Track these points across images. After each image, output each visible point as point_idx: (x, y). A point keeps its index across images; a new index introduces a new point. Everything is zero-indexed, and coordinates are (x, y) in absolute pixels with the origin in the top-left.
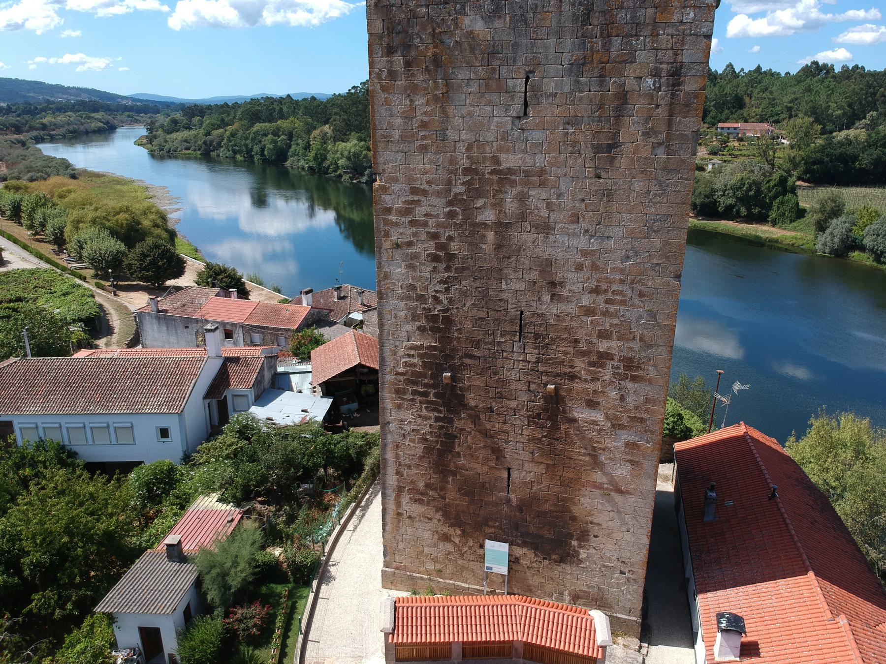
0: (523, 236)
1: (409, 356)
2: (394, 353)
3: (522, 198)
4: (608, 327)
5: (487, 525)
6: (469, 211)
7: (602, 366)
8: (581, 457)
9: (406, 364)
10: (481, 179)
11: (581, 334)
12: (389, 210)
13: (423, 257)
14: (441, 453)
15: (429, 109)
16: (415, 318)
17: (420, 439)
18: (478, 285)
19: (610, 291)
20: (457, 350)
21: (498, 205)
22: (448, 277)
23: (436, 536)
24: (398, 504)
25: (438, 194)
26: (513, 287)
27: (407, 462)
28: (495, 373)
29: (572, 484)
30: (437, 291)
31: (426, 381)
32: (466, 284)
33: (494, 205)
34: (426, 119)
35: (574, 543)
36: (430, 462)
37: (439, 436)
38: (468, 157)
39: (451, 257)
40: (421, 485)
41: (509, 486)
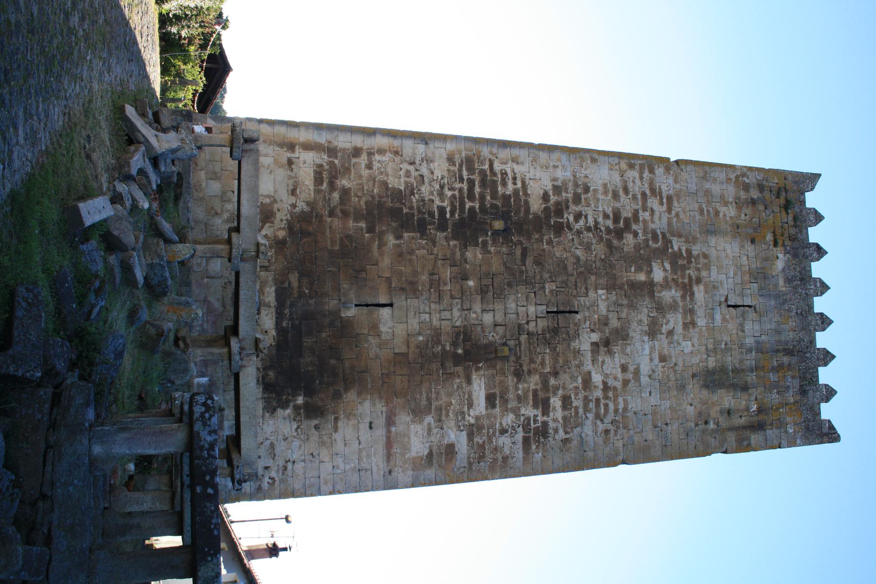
1: (515, 179)
2: (515, 160)
3: (674, 307)
4: (574, 405)
5: (302, 275)
7: (535, 406)
8: (424, 395)
9: (504, 174)
11: (565, 377)
12: (652, 171)
13: (618, 205)
14: (395, 213)
15: (728, 218)
16: (557, 189)
17: (412, 185)
18: (598, 264)
19: (607, 401)
20: (529, 238)
21: (666, 285)
22: (601, 231)
23: (267, 201)
24: (308, 147)
25: (669, 224)
26: (600, 300)
27: (376, 165)
28: (510, 285)
29: (386, 390)
30: (586, 217)
31: (488, 198)
32: (599, 250)
33: (666, 279)
34: (721, 215)
35: (300, 400)
36: (380, 197)
37: (420, 211)
38: (698, 255)
39: (619, 234)
40: (344, 182)
41: (367, 305)
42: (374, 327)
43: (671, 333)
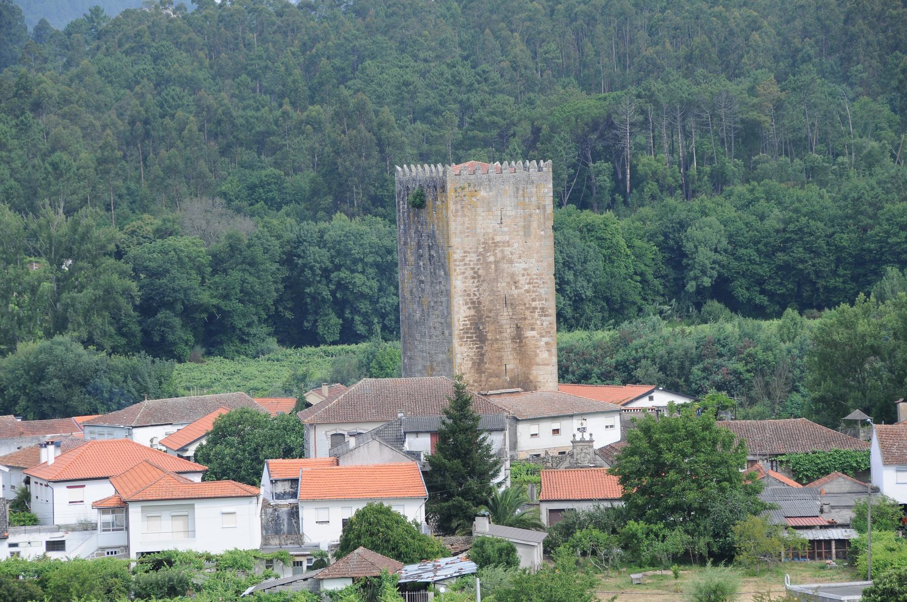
0: (505, 266)
3: (502, 251)
6: (484, 257)
10: (489, 245)
11: (526, 301)
12: (455, 260)
14: (479, 364)
26: (502, 285)
32: (485, 285)
39: (479, 276)
40: (471, 382)
42: (512, 370)
43: (512, 254)
